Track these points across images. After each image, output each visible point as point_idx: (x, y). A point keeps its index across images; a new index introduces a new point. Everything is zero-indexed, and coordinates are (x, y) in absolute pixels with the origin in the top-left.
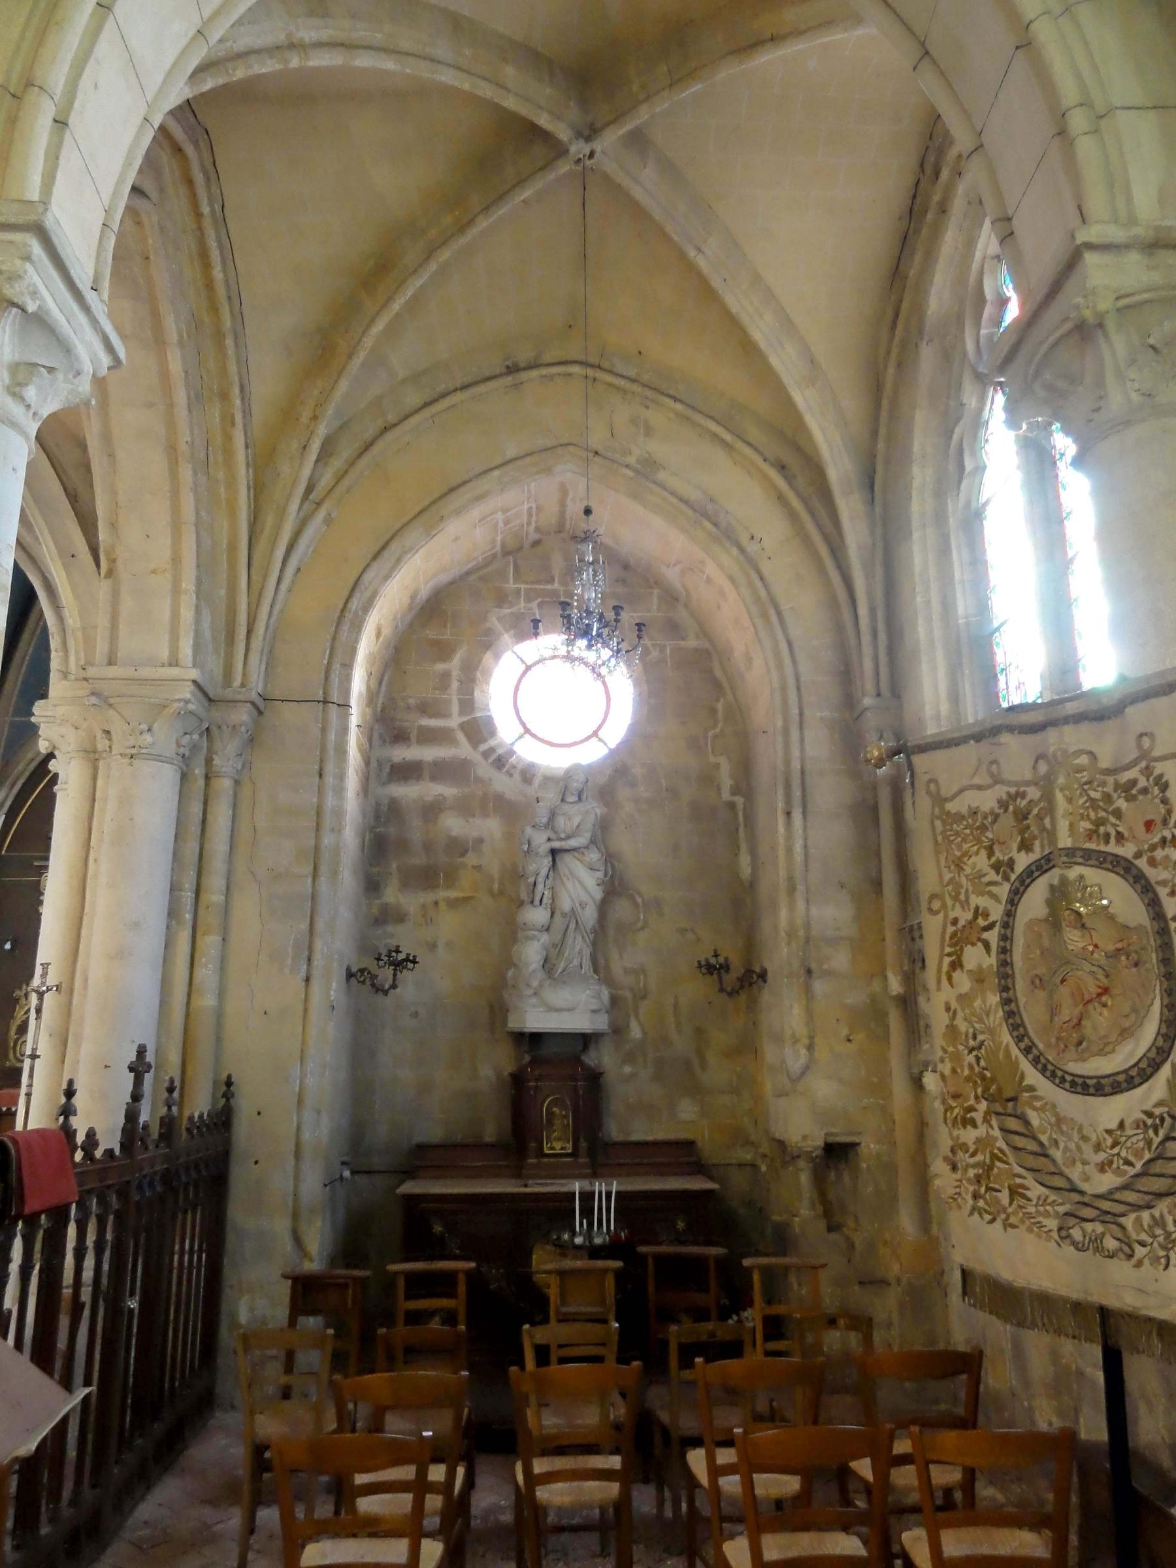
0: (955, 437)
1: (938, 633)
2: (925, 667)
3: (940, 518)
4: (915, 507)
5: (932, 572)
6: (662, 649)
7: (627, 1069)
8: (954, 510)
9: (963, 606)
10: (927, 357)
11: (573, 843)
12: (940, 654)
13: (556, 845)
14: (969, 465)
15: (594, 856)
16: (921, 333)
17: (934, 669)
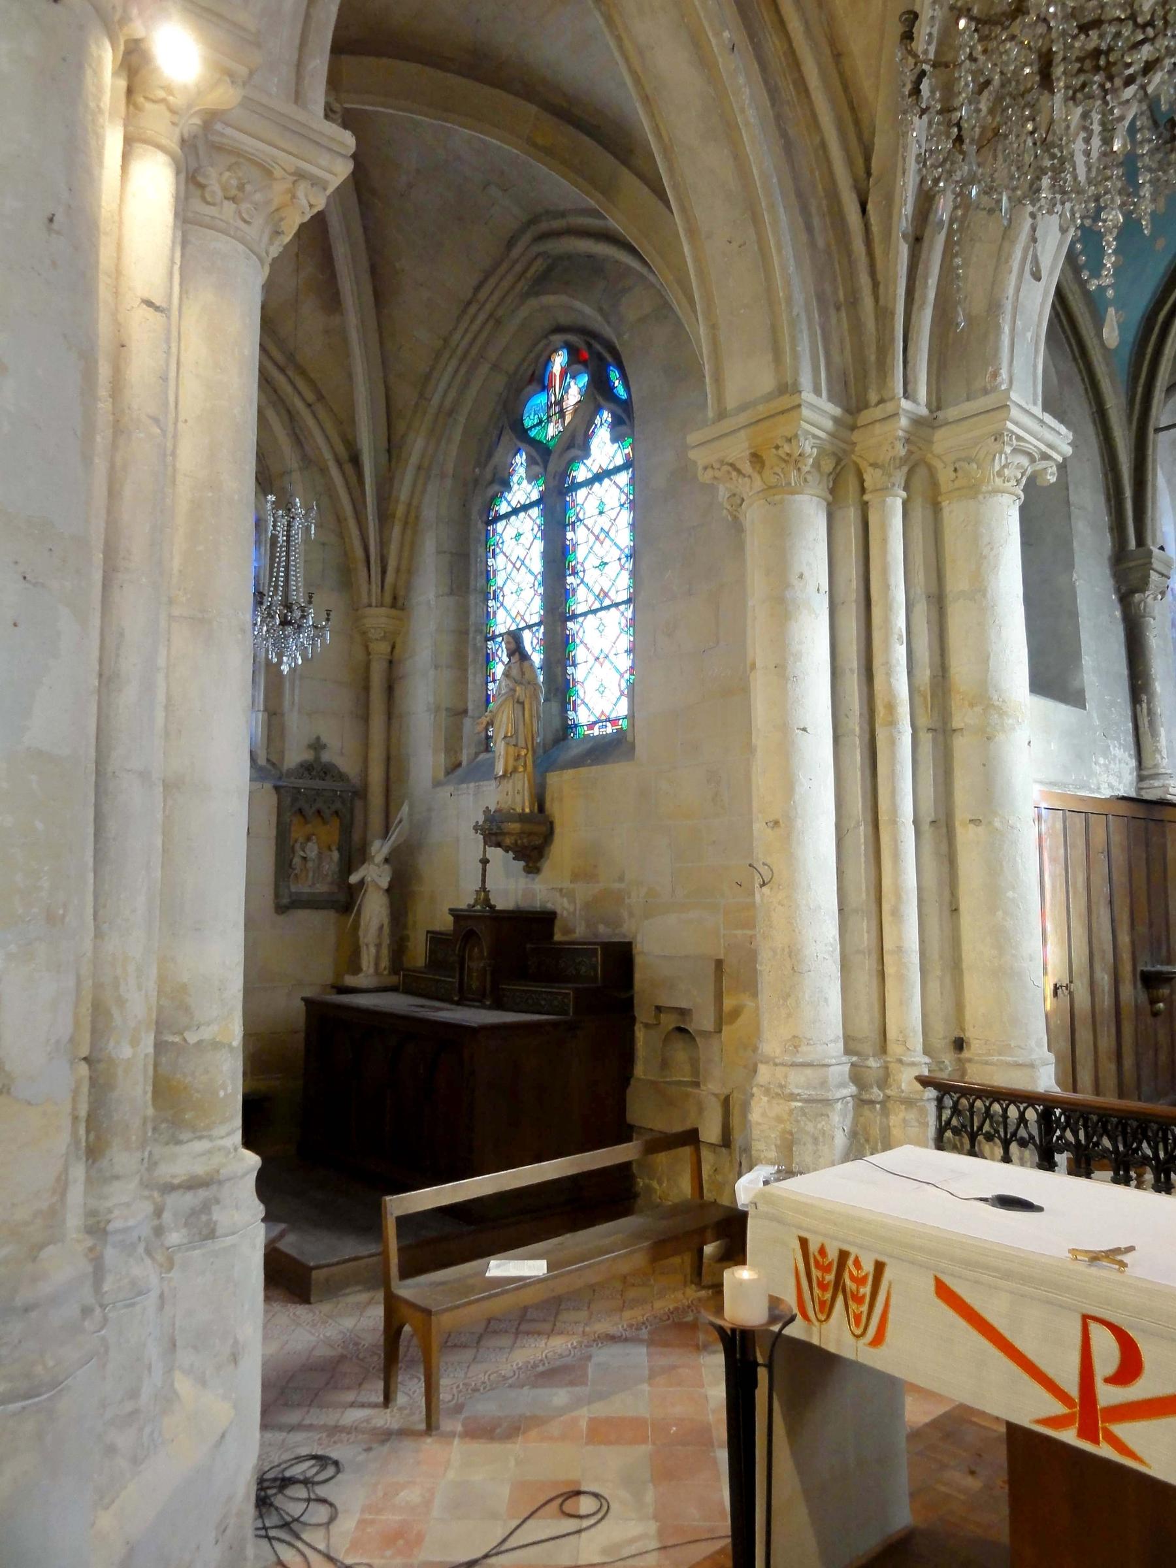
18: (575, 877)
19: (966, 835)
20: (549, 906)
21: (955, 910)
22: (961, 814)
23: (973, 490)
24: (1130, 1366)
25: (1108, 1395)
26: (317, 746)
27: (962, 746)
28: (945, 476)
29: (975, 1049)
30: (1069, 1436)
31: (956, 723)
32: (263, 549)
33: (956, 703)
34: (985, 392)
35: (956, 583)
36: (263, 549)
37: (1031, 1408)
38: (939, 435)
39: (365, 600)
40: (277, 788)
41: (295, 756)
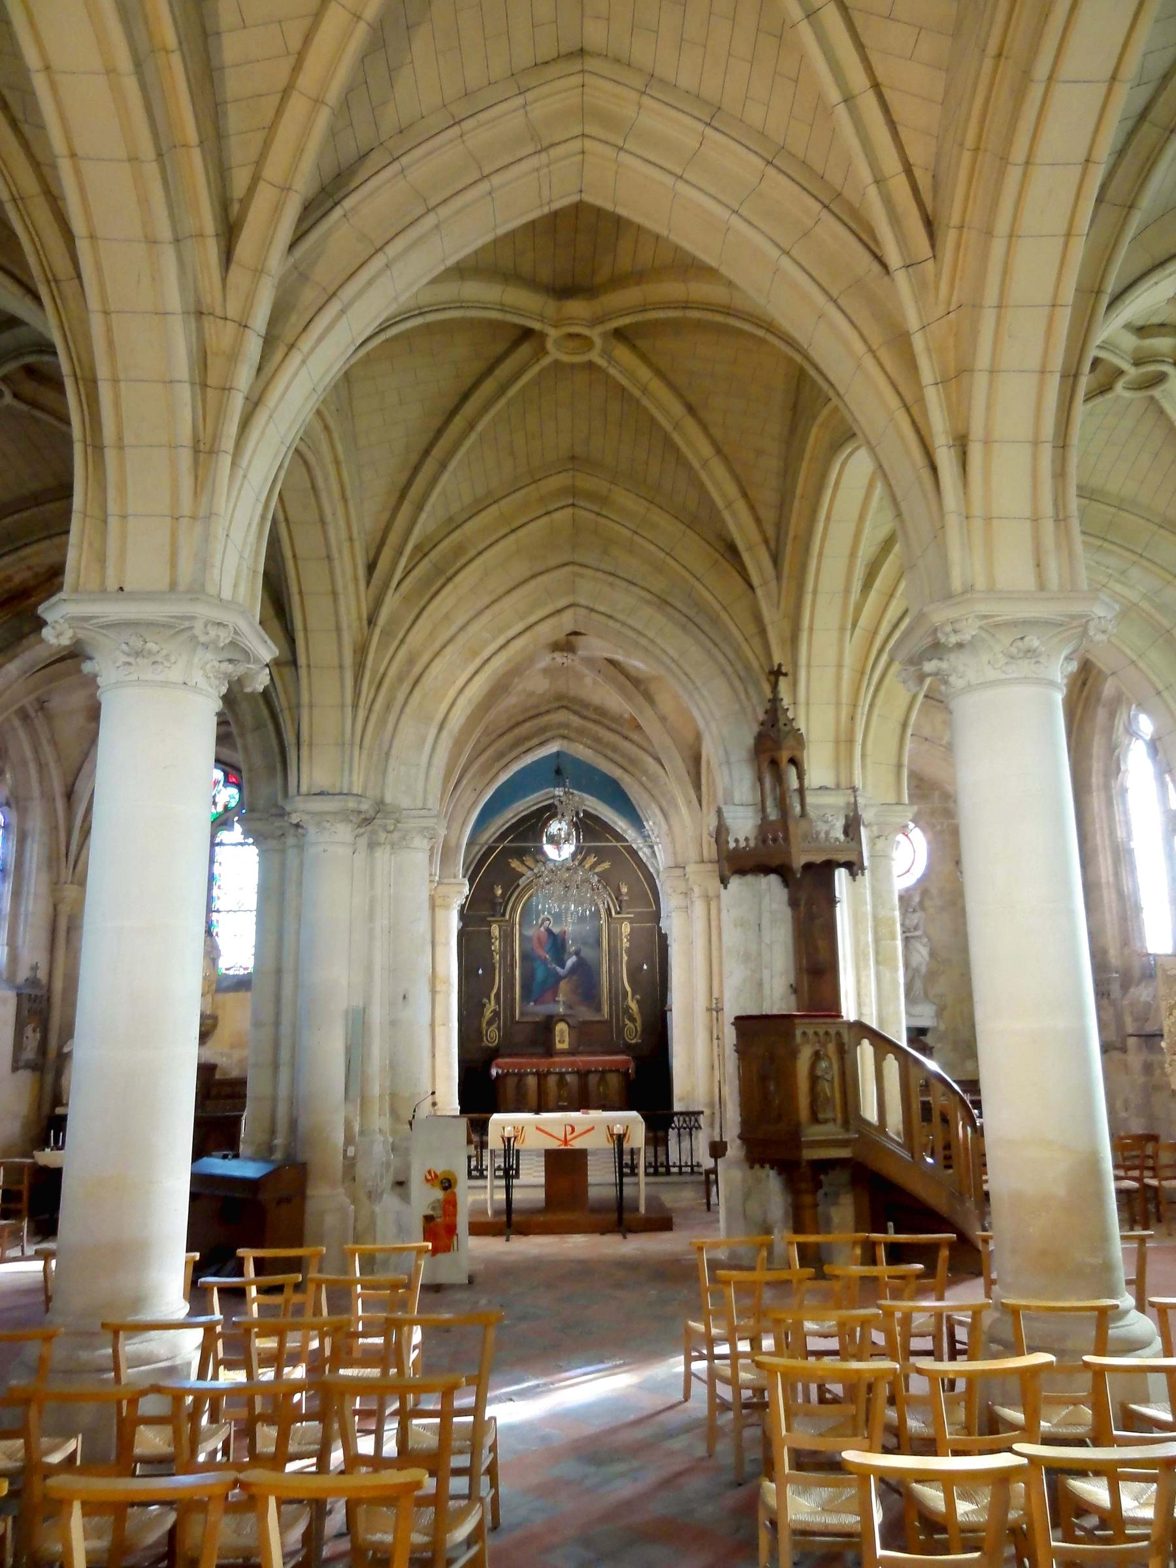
0: (1116, 753)
1: (1107, 843)
2: (1101, 858)
3: (1107, 787)
4: (1094, 780)
5: (1104, 814)
6: (942, 824)
7: (939, 1045)
8: (1115, 785)
9: (1120, 833)
10: (1101, 714)
11: (917, 933)
12: (1109, 854)
13: (908, 934)
14: (1123, 767)
15: (925, 940)
16: (1098, 700)
17: (1106, 860)
18: (232, 1047)
19: (439, 1030)
20: (212, 1061)
21: (434, 1056)
22: (438, 1021)
23: (447, 907)
24: (573, 1130)
25: (569, 1137)
26: (35, 968)
27: (439, 998)
28: (438, 902)
29: (439, 1105)
30: (563, 1147)
31: (438, 988)
32: (10, 844)
33: (437, 982)
34: (455, 877)
35: (440, 938)
36: (10, 844)
37: (554, 1145)
38: (440, 887)
39: (62, 879)
40: (19, 995)
41: (23, 974)
